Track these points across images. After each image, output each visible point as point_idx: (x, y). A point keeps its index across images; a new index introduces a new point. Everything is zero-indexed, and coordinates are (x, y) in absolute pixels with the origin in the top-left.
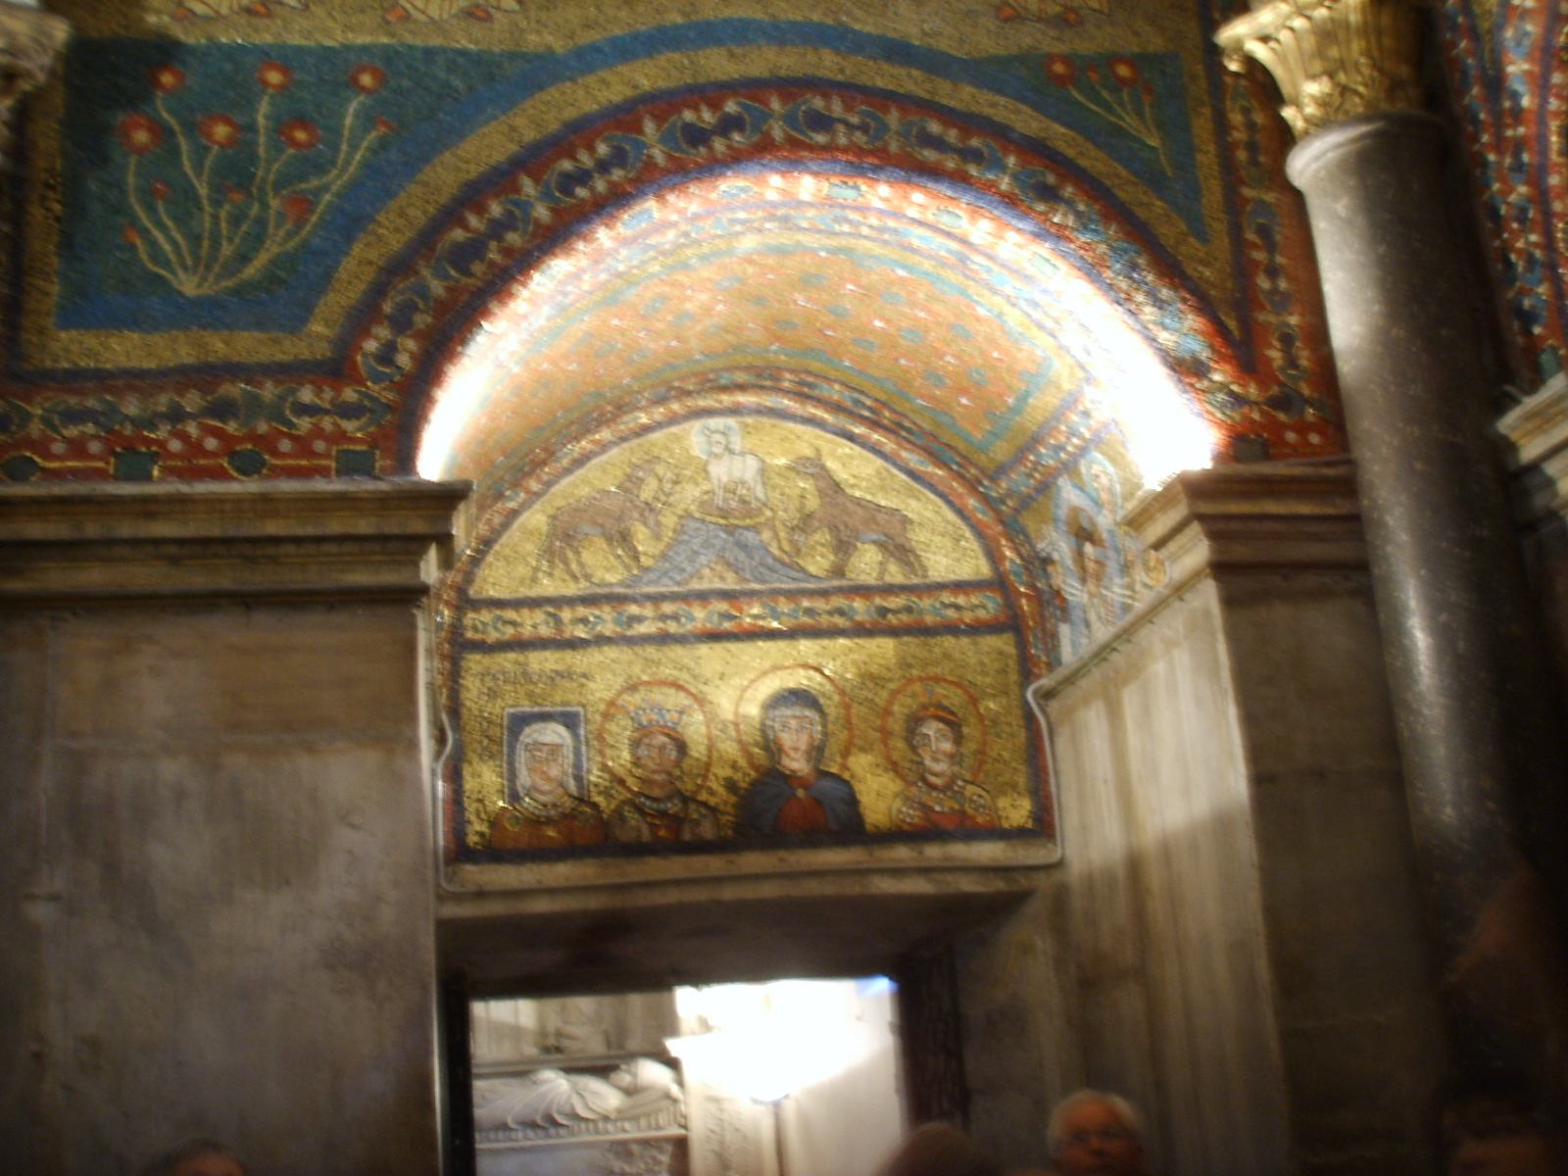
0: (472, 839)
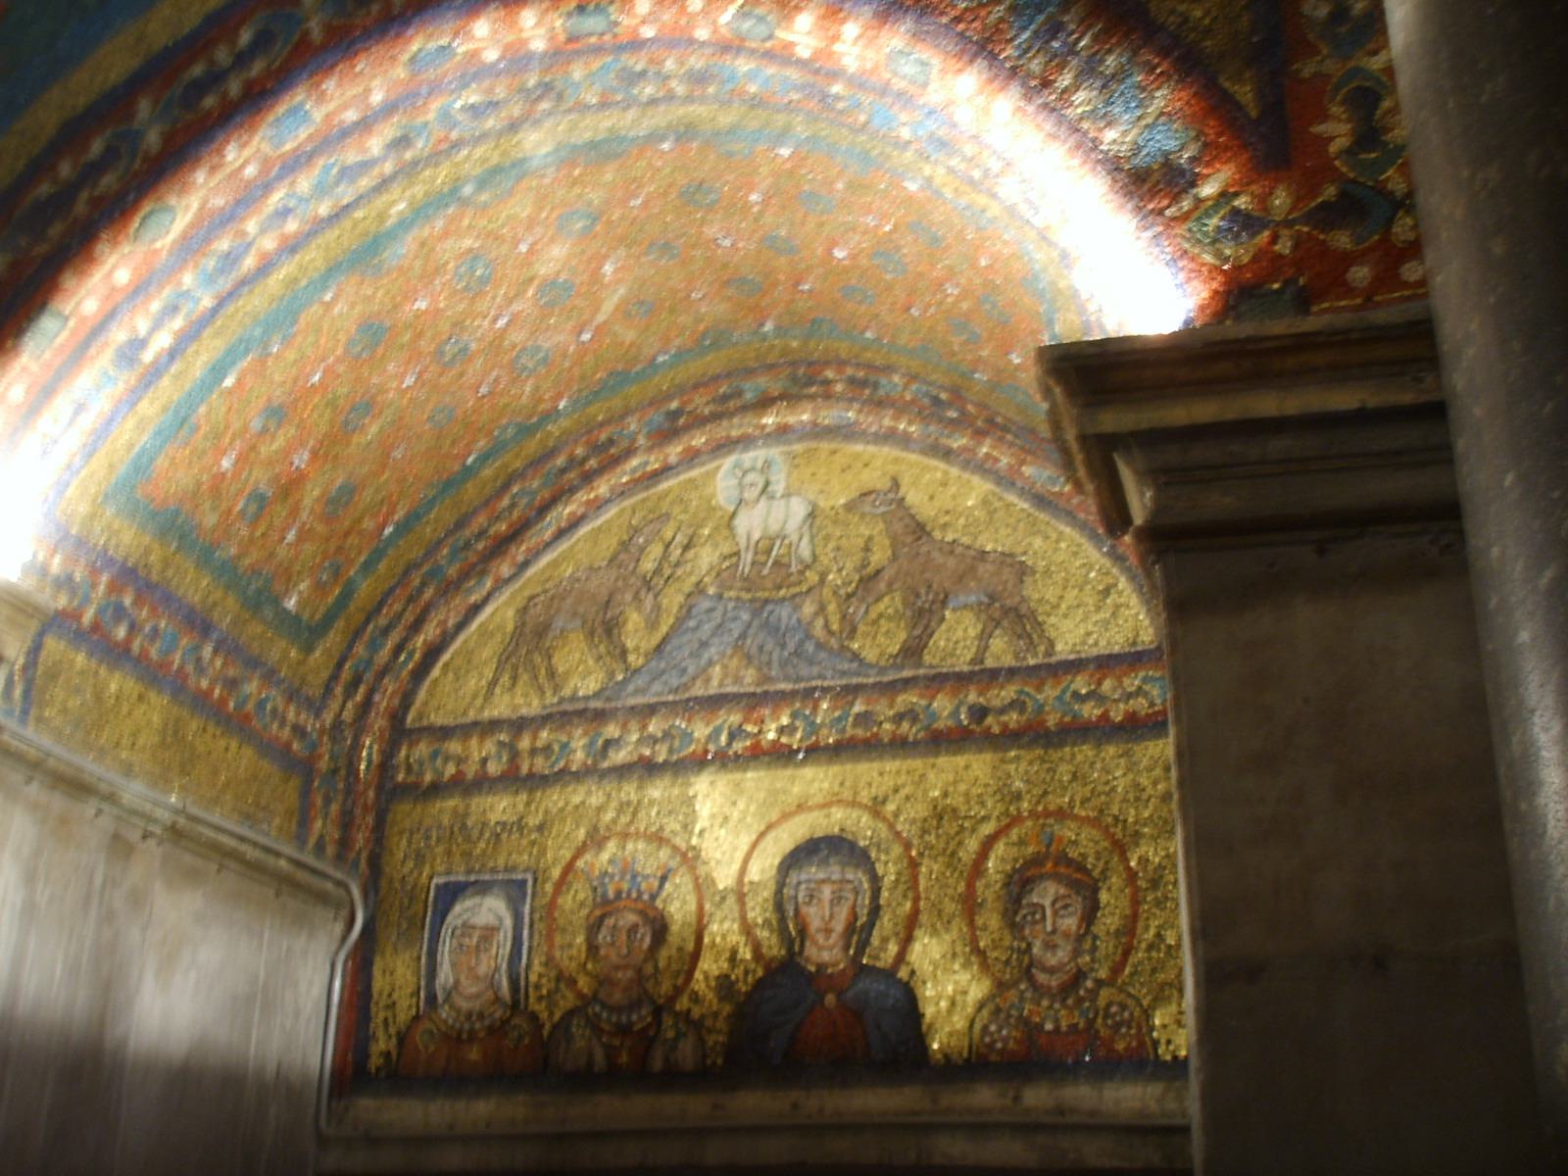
0: (375, 1062)
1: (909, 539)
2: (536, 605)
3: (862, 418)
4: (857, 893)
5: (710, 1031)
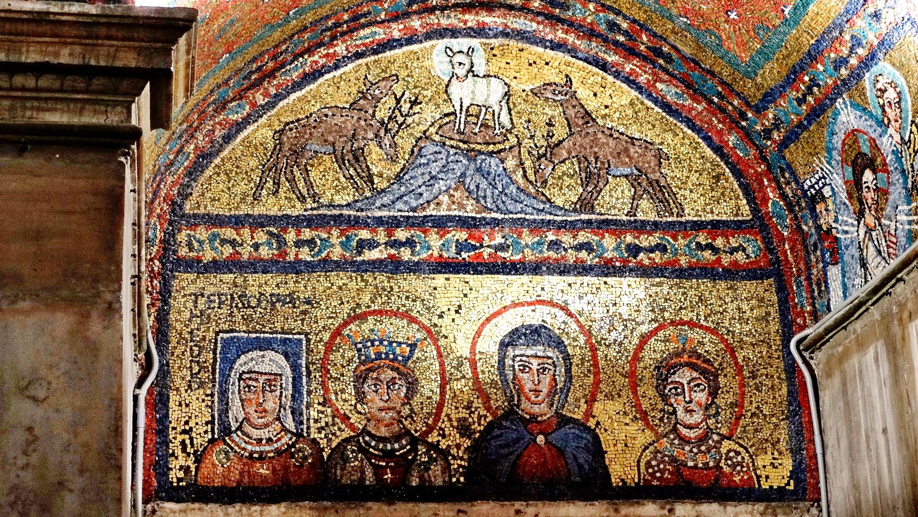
0: (174, 475)
1: (580, 123)
2: (291, 129)
3: (541, 27)
4: (555, 367)
5: (454, 458)
